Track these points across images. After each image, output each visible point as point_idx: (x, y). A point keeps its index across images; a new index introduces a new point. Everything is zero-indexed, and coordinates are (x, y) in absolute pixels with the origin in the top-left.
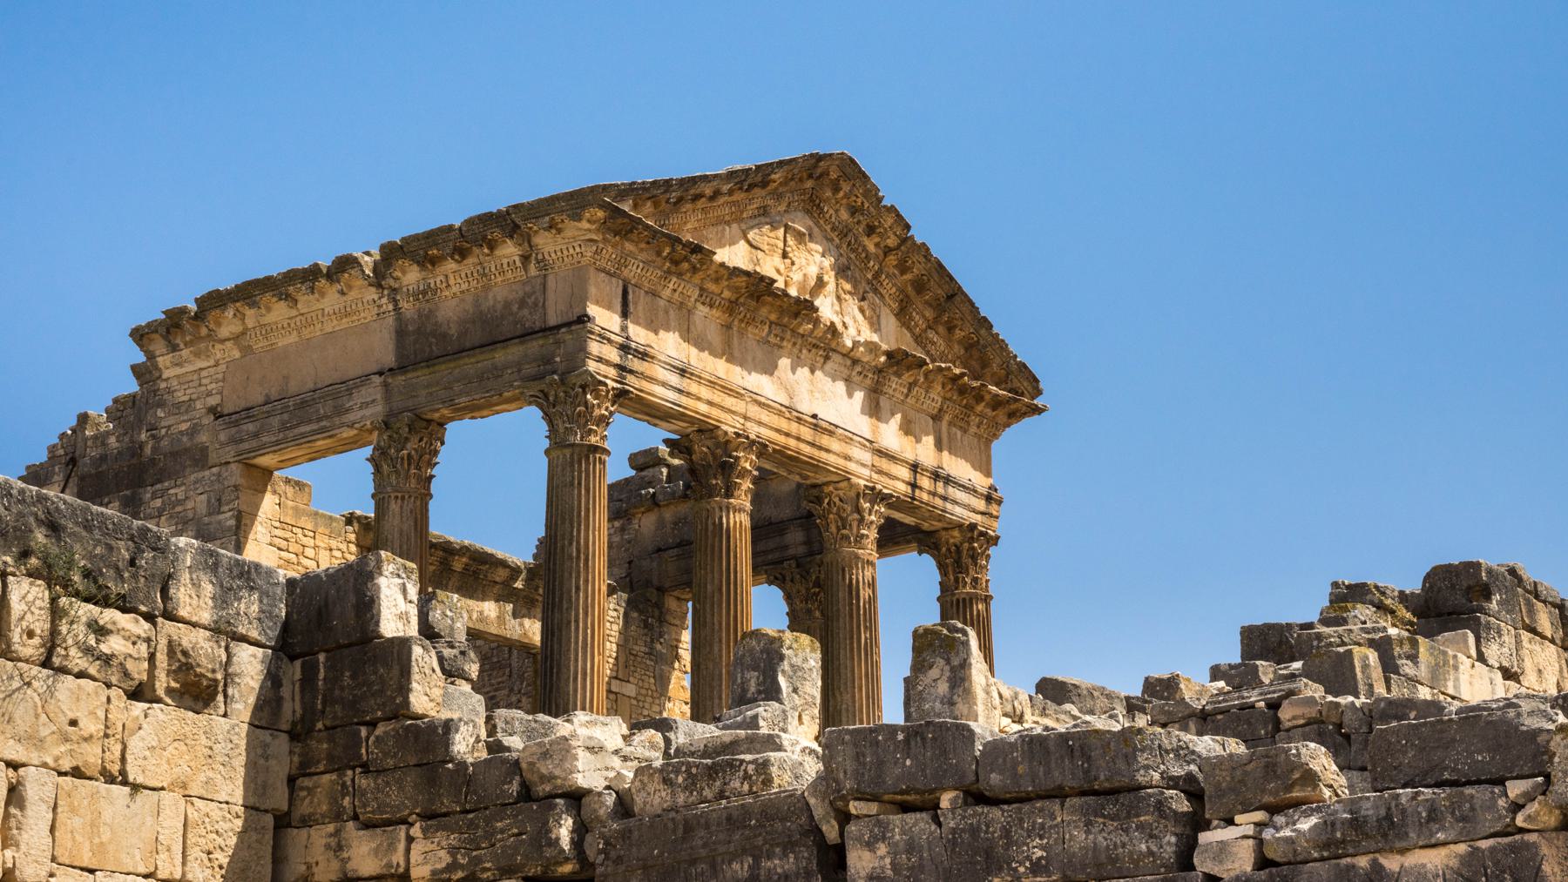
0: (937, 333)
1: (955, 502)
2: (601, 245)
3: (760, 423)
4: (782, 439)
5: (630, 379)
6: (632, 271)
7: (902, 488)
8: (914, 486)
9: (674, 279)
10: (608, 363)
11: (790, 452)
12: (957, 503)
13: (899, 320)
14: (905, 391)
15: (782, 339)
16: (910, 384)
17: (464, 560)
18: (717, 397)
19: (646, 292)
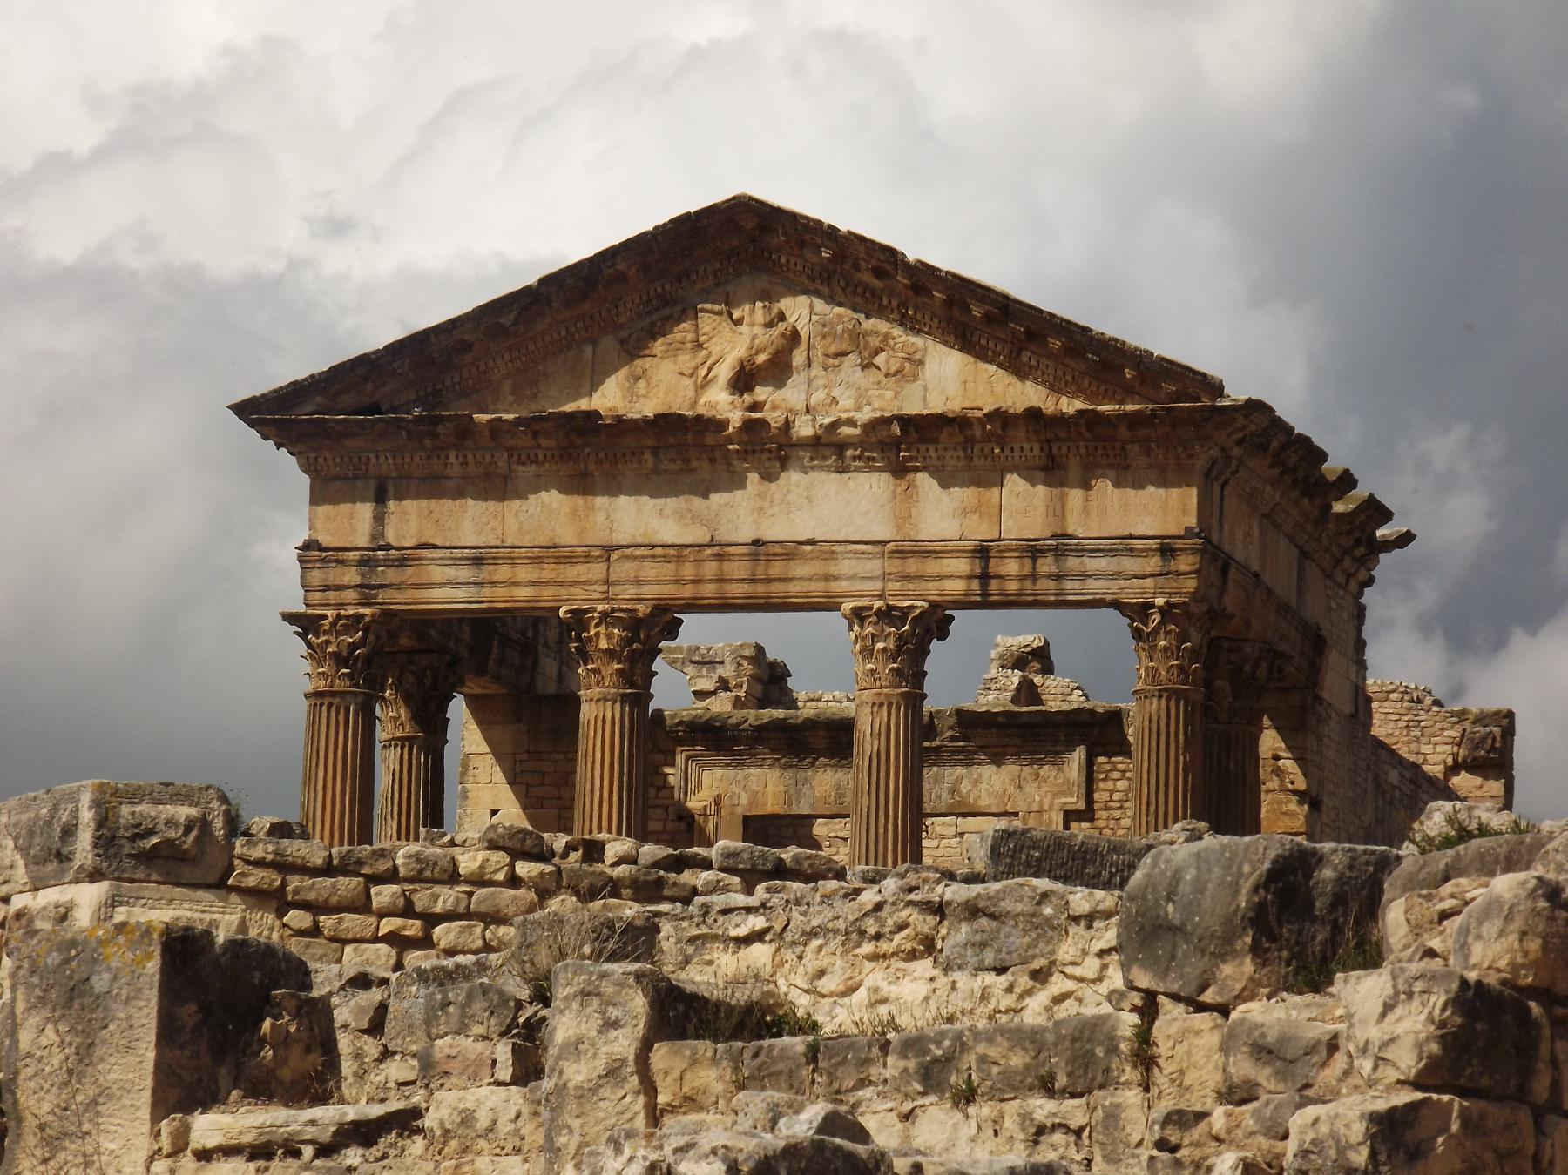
0: (1033, 353)
1: (1084, 576)
2: (312, 455)
3: (638, 582)
4: (688, 589)
5: (382, 596)
6: (386, 465)
7: (956, 587)
8: (985, 577)
9: (452, 455)
10: (340, 588)
11: (706, 601)
12: (1090, 576)
13: (968, 353)
14: (961, 454)
15: (687, 461)
16: (966, 442)
17: (821, 733)
18: (547, 573)
19: (423, 479)
